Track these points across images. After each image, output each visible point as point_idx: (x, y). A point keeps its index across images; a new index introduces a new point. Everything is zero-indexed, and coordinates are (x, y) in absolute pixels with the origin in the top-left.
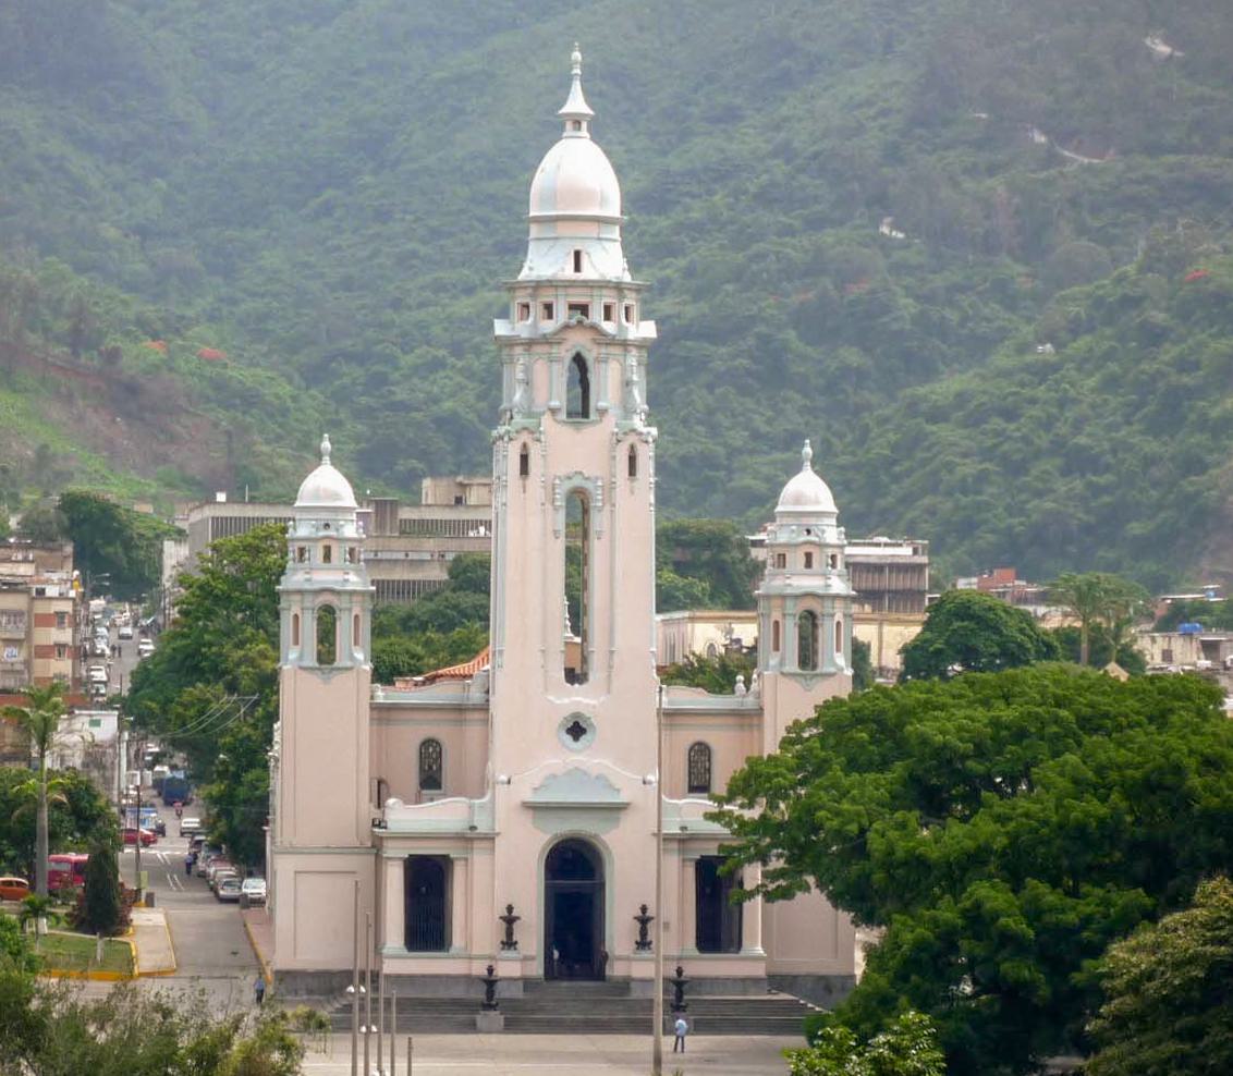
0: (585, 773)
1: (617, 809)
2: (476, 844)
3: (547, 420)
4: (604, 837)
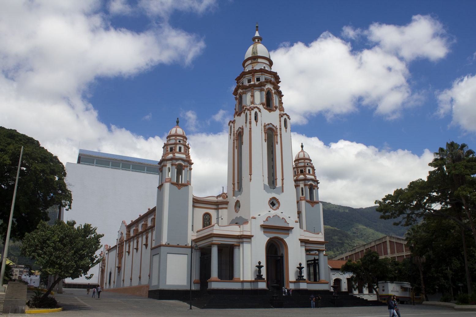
0: (279, 217)
1: (288, 230)
2: (245, 240)
3: (261, 107)
4: (285, 239)
